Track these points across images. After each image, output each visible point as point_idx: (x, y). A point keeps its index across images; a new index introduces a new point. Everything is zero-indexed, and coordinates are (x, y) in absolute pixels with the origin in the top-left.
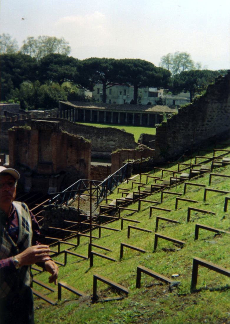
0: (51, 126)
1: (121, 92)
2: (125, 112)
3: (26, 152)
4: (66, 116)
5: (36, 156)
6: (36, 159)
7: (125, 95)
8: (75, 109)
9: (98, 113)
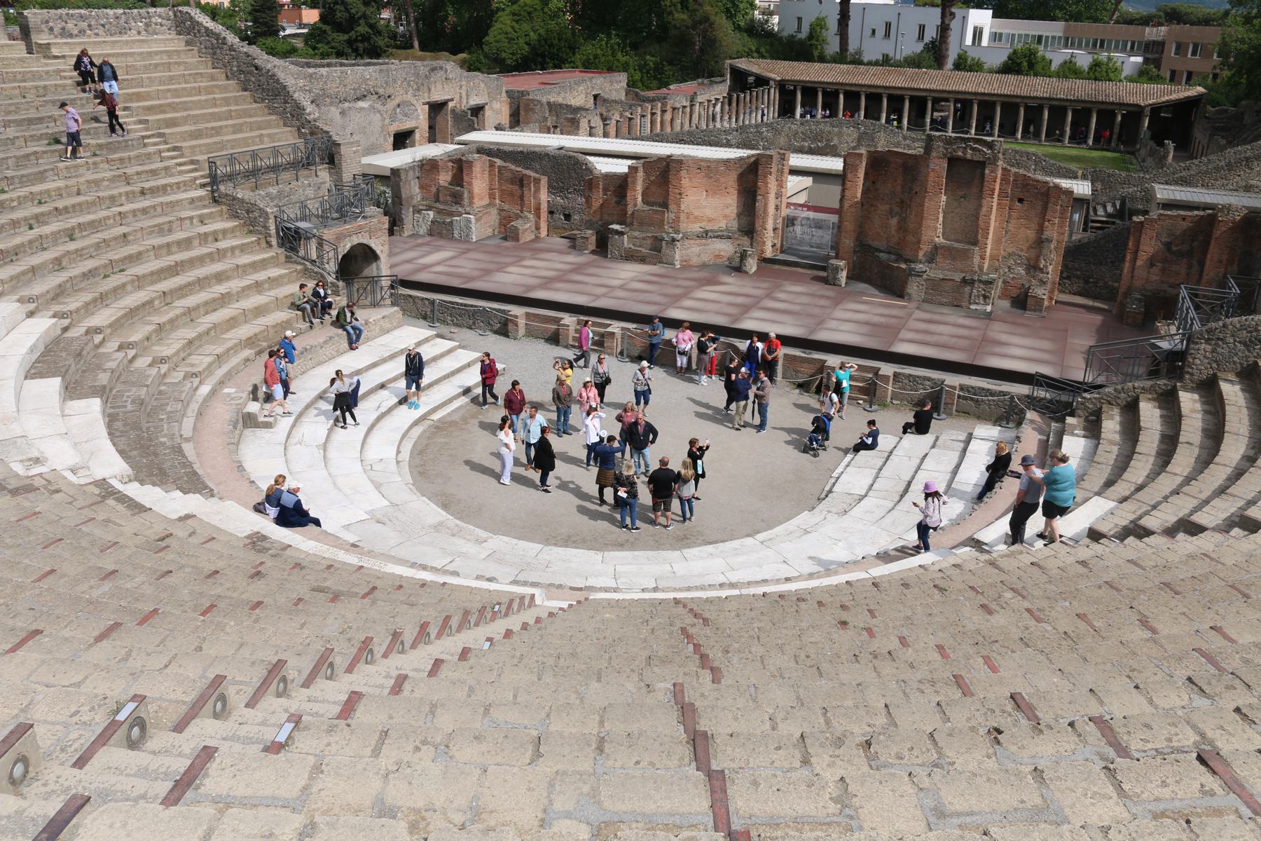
8: (772, 83)
9: (841, 96)
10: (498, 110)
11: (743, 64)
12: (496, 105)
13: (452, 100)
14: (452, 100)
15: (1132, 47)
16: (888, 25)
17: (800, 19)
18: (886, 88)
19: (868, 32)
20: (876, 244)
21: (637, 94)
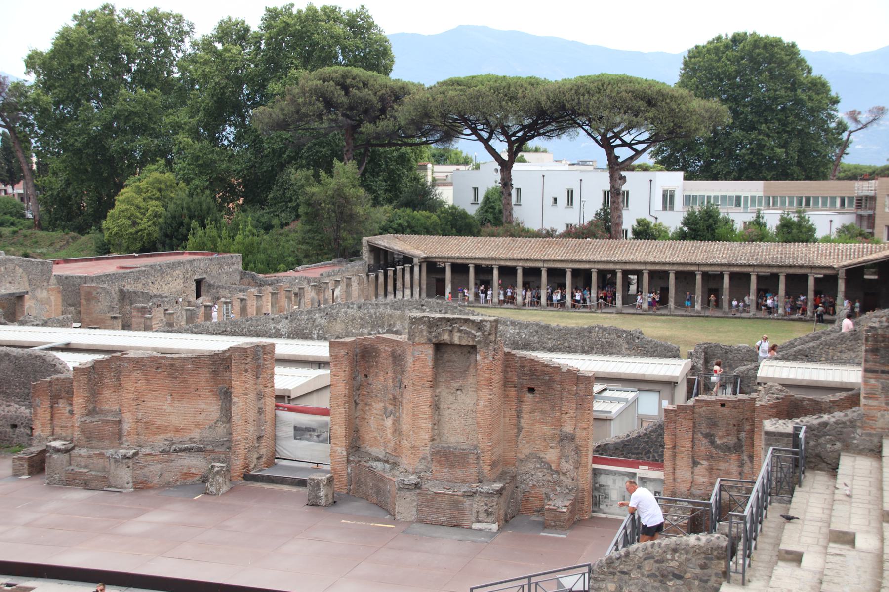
0: (473, 332)
2: (587, 266)
4: (390, 288)
8: (416, 261)
9: (496, 273)
10: (45, 298)
11: (386, 241)
12: (42, 294)
15: (843, 204)
16: (570, 194)
17: (476, 190)
18: (544, 261)
19: (549, 201)
21: (253, 277)
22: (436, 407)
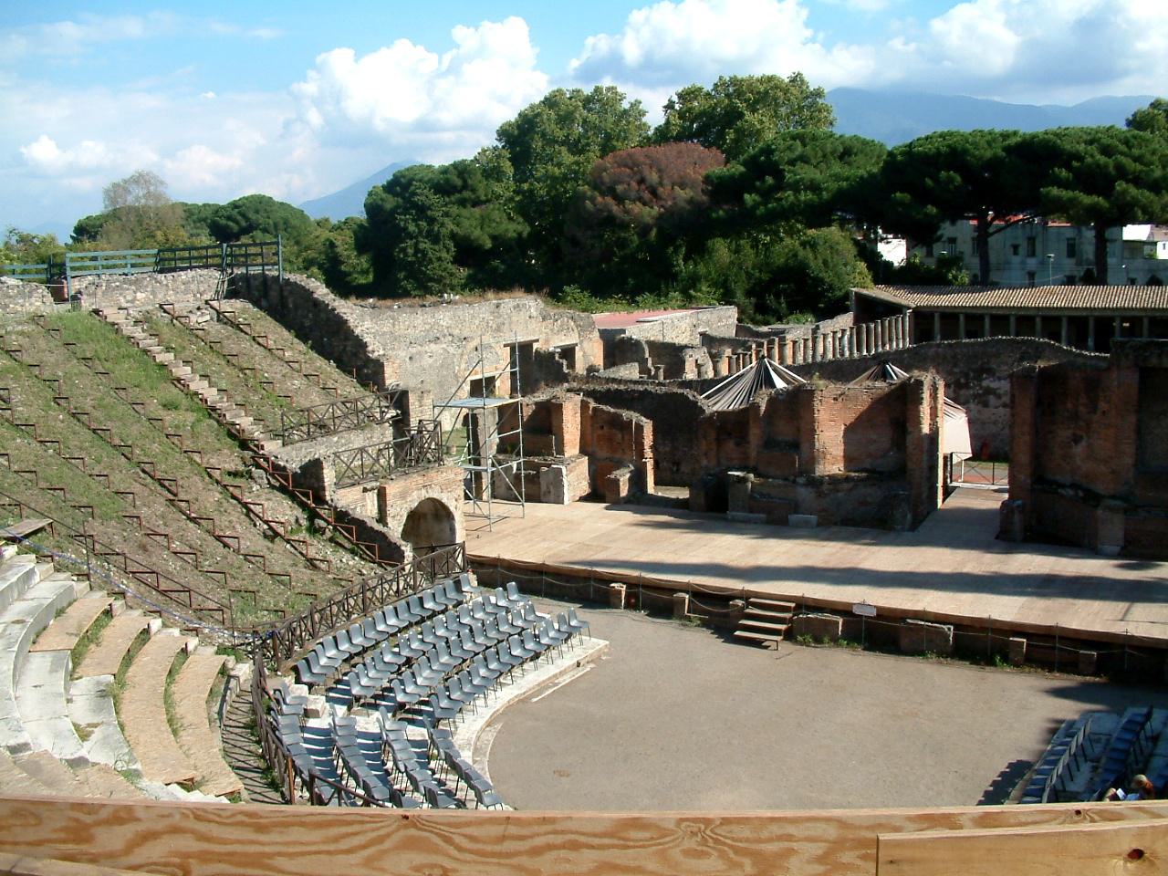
1: (1016, 248)
3: (1077, 440)
5: (1129, 449)
6: (1128, 461)
7: (1032, 254)
9: (987, 321)
13: (537, 341)
14: (537, 341)
20: (1059, 478)
22: (1138, 431)
